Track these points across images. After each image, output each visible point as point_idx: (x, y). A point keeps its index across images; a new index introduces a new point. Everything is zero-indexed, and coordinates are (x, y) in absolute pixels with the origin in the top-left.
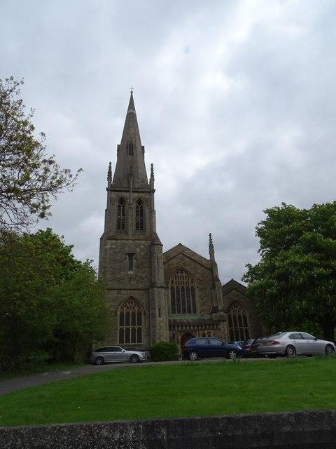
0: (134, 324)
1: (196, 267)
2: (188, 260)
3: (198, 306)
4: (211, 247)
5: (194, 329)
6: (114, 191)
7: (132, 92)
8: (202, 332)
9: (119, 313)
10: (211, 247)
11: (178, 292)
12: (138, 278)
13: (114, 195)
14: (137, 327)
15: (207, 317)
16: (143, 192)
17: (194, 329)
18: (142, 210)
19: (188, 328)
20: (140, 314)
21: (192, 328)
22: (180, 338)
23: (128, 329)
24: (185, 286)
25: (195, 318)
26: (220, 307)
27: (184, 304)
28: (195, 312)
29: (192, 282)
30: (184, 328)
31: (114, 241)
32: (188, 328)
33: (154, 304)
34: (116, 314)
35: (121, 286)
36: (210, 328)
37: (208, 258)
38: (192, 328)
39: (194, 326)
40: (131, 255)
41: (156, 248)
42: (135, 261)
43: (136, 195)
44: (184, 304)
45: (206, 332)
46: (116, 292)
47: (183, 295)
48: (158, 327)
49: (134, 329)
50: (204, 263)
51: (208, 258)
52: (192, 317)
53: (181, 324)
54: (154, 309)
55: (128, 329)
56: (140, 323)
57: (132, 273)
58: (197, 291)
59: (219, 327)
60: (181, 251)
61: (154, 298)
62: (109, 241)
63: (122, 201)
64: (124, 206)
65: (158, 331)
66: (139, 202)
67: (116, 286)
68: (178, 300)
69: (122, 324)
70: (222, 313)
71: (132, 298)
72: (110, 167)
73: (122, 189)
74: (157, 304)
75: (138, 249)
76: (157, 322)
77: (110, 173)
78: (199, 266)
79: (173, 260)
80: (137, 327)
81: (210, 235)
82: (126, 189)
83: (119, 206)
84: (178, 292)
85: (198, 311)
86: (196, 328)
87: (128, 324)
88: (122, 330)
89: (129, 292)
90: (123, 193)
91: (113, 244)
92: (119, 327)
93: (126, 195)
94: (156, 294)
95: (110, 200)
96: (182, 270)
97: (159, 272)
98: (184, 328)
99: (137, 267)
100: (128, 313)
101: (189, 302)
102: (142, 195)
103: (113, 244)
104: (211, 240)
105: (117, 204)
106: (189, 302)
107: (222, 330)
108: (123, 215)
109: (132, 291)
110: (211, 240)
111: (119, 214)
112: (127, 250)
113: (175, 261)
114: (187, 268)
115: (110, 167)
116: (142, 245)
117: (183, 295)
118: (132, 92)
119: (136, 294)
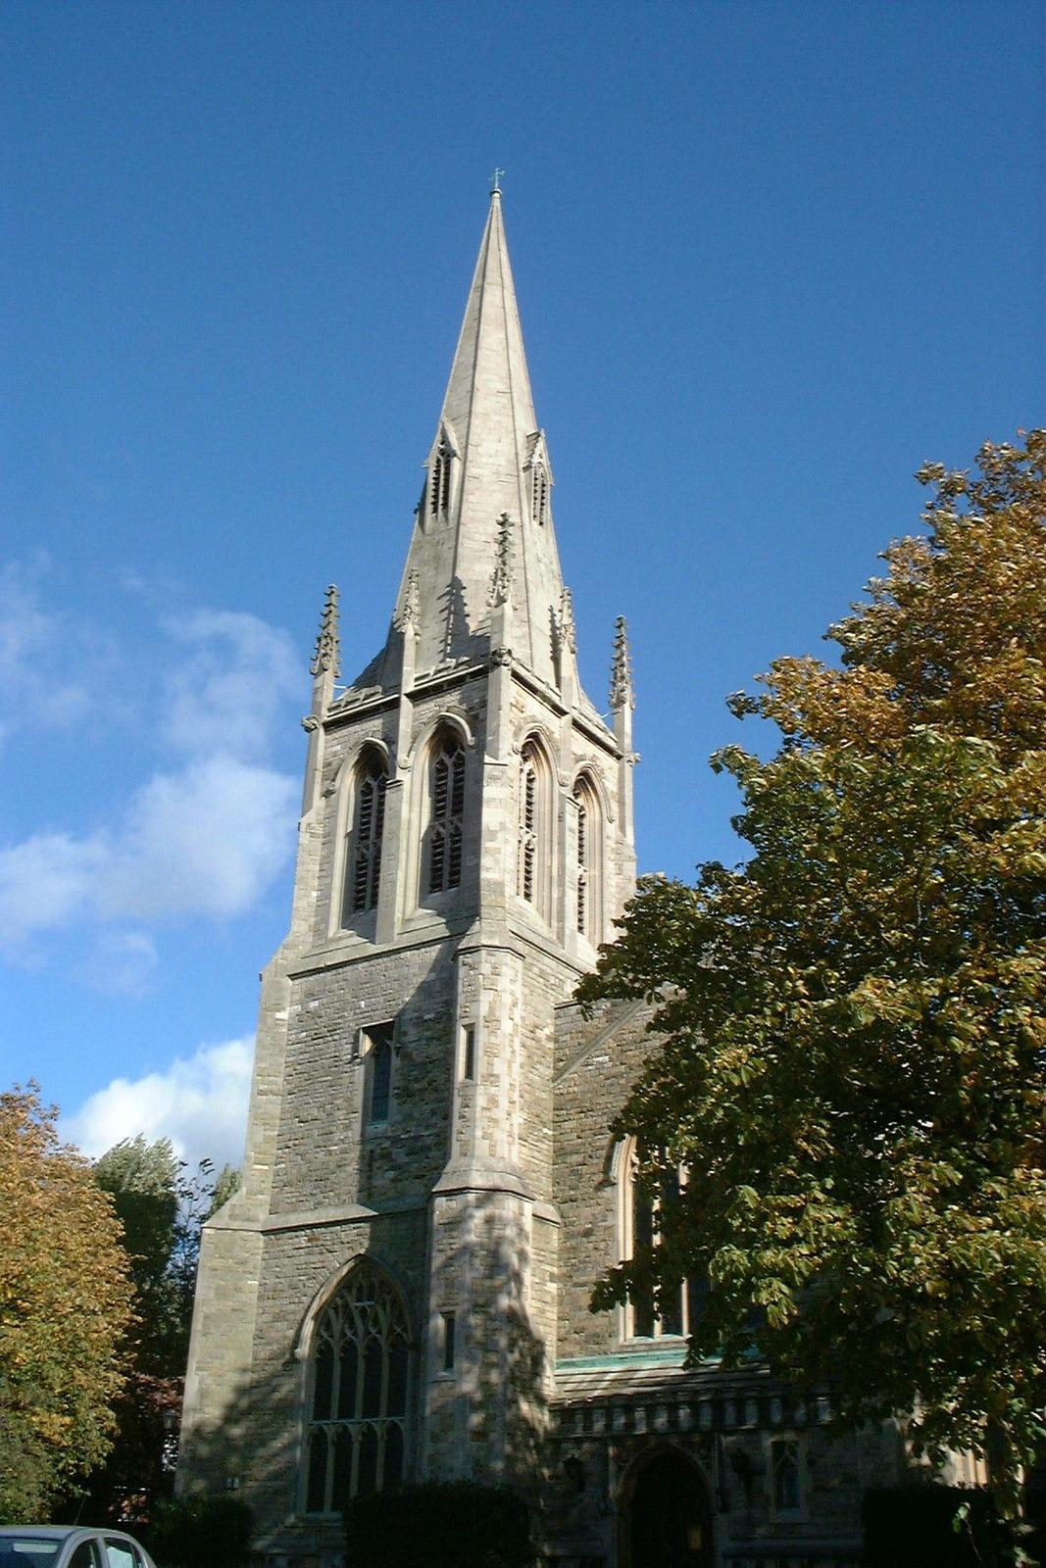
12: (399, 1154)
19: (661, 1421)
20: (397, 1343)
23: (344, 1437)
36: (788, 1422)
40: (378, 1033)
42: (396, 1062)
46: (302, 1239)
49: (369, 1435)
66: (445, 738)
91: (310, 995)
105: (348, 784)
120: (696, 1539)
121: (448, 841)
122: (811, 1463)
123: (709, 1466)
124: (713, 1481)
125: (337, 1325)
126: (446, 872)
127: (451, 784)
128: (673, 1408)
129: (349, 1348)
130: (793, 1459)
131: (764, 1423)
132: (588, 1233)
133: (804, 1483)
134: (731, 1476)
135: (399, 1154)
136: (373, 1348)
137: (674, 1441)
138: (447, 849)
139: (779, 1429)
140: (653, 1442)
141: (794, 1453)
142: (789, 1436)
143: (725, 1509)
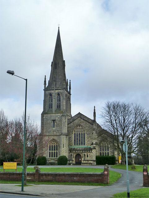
0: (54, 150)
1: (86, 124)
2: (83, 120)
3: (86, 141)
4: (95, 113)
6: (47, 90)
8: (84, 153)
9: (49, 145)
10: (95, 113)
11: (77, 135)
12: (56, 131)
14: (56, 151)
15: (89, 146)
16: (60, 89)
18: (60, 98)
20: (57, 146)
21: (80, 152)
22: (74, 156)
23: (52, 152)
24: (81, 133)
25: (84, 147)
26: (94, 143)
27: (80, 141)
28: (84, 144)
29: (84, 131)
30: (76, 152)
31: (47, 115)
33: (61, 142)
34: (48, 146)
35: (50, 134)
36: (88, 152)
37: (93, 119)
38: (80, 152)
39: (81, 151)
40: (54, 121)
42: (55, 123)
43: (57, 91)
44: (80, 141)
45: (86, 153)
47: (80, 137)
48: (62, 152)
49: (54, 152)
51: (93, 119)
52: (82, 147)
53: (76, 150)
54: (61, 144)
55: (52, 152)
56: (57, 150)
57: (54, 128)
58: (86, 134)
59: (92, 151)
60: (80, 115)
61: (61, 140)
62: (45, 115)
63: (51, 95)
64: (52, 97)
65: (62, 153)
66: (59, 94)
67: (47, 134)
68: (77, 139)
69: (50, 150)
70: (95, 145)
71: (54, 139)
74: (62, 142)
75: (57, 118)
76: (62, 150)
77: (45, 81)
78: (87, 123)
79: (76, 121)
80: (56, 151)
81: (95, 107)
82: (53, 89)
84: (77, 135)
85: (86, 144)
86: (82, 152)
87: (52, 150)
88: (50, 152)
89: (52, 137)
90: (51, 91)
91: (46, 116)
92: (49, 151)
93: (52, 91)
94: (62, 138)
95: (45, 95)
96: (79, 125)
97: (64, 128)
99: (57, 126)
100: (52, 146)
101: (82, 140)
102: (59, 91)
103: (46, 116)
104: (95, 109)
106: (82, 140)
108: (52, 101)
109: (54, 137)
110: (95, 109)
112: (53, 118)
113: (76, 121)
114: (82, 124)
116: (59, 116)
117: (80, 137)
119: (55, 138)
124: (82, 156)
125: (51, 144)
129: (52, 146)
131: (86, 152)
133: (89, 156)
134: (84, 155)
135: (56, 131)
136: (54, 146)
142: (88, 153)
143: (83, 157)
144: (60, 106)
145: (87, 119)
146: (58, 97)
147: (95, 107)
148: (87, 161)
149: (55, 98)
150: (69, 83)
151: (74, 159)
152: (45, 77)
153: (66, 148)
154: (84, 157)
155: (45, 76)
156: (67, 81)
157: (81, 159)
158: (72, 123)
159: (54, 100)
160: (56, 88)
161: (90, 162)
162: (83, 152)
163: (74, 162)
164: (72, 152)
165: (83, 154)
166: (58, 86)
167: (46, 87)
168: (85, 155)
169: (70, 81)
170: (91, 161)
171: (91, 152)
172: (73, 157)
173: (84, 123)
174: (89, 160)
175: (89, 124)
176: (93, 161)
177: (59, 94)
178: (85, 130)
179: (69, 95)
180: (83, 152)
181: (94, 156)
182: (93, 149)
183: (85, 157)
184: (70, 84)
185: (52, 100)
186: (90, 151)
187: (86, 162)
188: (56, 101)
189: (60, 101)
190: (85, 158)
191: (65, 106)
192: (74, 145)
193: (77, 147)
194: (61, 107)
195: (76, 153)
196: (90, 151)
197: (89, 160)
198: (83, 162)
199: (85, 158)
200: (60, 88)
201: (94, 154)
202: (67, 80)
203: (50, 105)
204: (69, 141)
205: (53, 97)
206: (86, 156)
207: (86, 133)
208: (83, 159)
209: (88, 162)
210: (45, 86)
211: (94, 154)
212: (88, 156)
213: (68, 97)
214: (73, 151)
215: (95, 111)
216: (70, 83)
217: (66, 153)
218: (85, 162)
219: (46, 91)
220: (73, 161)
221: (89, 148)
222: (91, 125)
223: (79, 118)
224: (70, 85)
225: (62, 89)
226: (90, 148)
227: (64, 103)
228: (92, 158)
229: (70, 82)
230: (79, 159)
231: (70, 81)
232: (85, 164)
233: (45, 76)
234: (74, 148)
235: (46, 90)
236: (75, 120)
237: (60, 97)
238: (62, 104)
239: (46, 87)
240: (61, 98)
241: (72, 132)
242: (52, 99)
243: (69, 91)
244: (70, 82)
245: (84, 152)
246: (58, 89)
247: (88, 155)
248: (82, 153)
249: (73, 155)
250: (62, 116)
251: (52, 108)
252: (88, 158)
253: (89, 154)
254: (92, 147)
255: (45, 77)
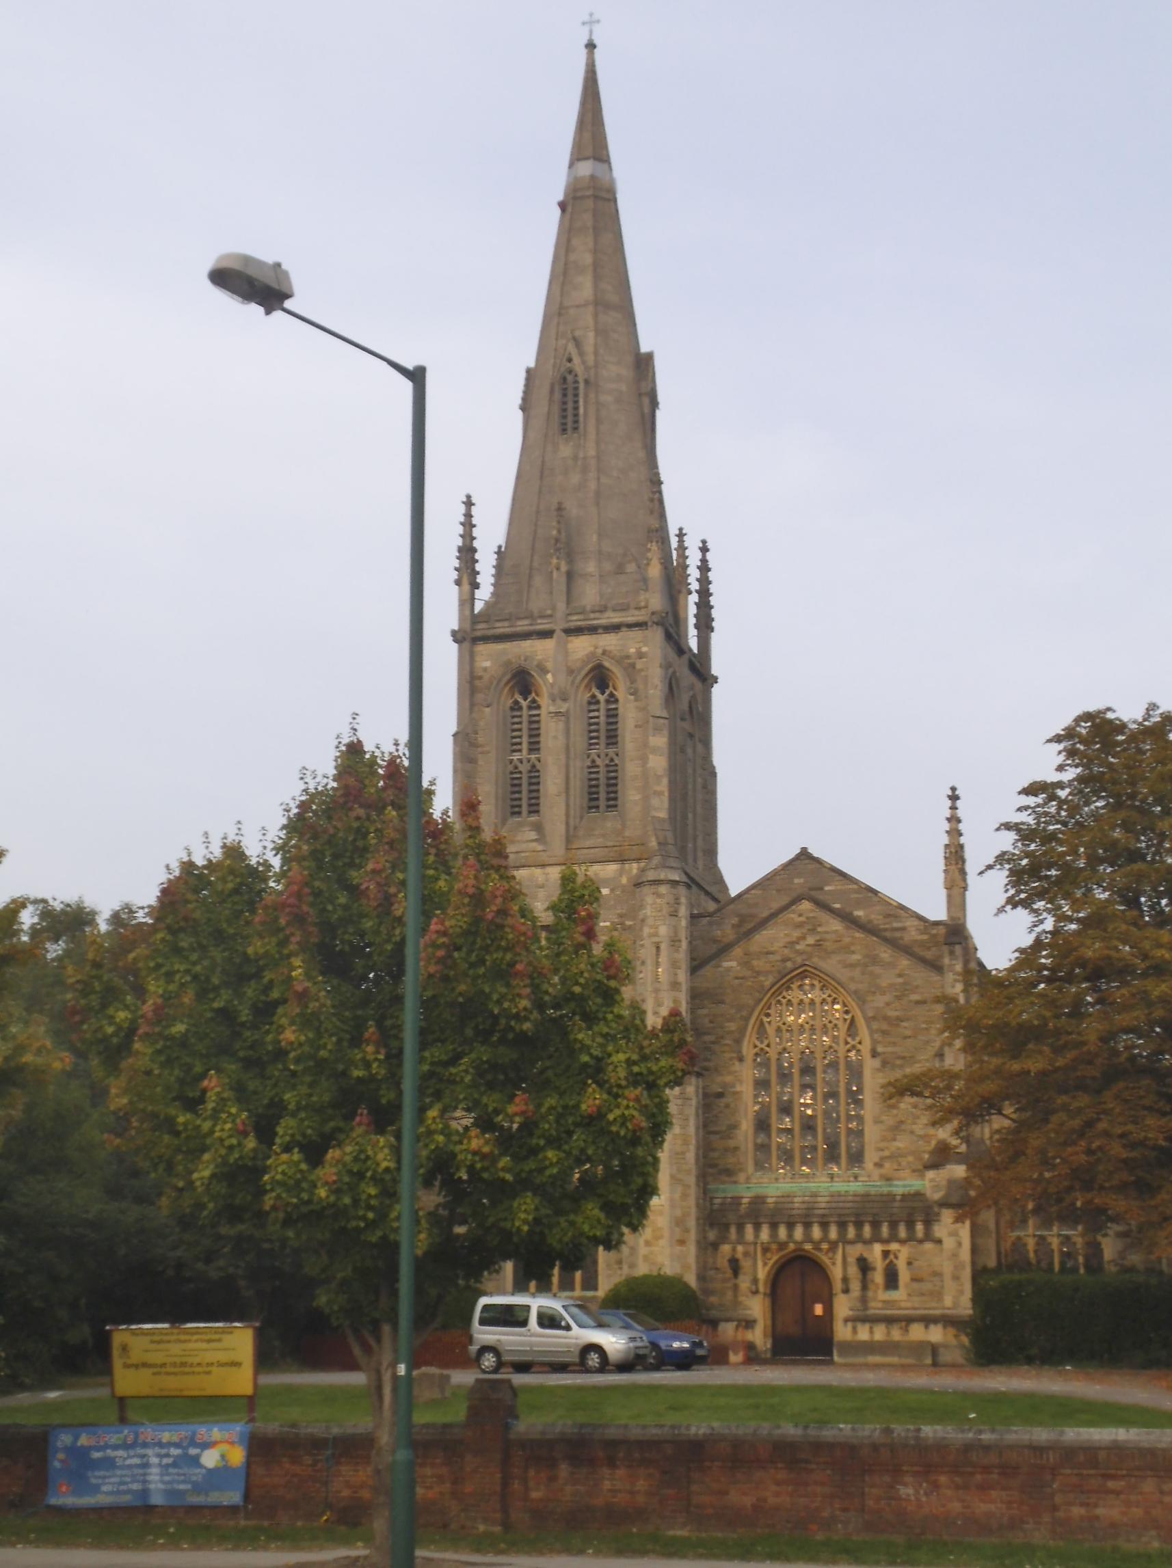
1: (874, 960)
2: (836, 925)
3: (872, 1134)
5: (825, 1238)
6: (486, 639)
7: (591, 46)
8: (856, 1250)
13: (488, 658)
15: (907, 1183)
17: (825, 1238)
18: (612, 715)
19: (799, 1233)
21: (816, 1232)
22: (762, 1273)
25: (855, 1187)
28: (857, 1158)
30: (782, 1232)
32: (799, 1233)
36: (893, 1237)
38: (816, 1232)
39: (824, 1226)
41: (649, 899)
43: (581, 646)
45: (878, 1248)
50: (912, 934)
51: (935, 909)
52: (839, 1186)
59: (939, 1230)
64: (535, 705)
66: (600, 678)
72: (468, 524)
73: (523, 626)
78: (885, 954)
81: (954, 797)
82: (543, 625)
83: (516, 706)
85: (871, 1157)
86: (833, 1233)
90: (527, 645)
93: (541, 649)
98: (782, 1232)
102: (609, 641)
104: (954, 819)
107: (949, 1243)
108: (534, 747)
110: (954, 819)
111: (515, 747)
113: (774, 937)
114: (831, 965)
115: (468, 524)
118: (591, 46)
120: (819, 1310)
121: (602, 770)
122: (909, 1263)
123: (834, 1264)
124: (837, 1273)
126: (603, 796)
127: (603, 719)
128: (807, 1226)
130: (895, 1261)
131: (876, 1238)
132: (720, 1095)
133: (904, 1275)
134: (853, 1271)
137: (808, 1247)
138: (602, 776)
139: (887, 1241)
140: (792, 1246)
141: (896, 1257)
142: (894, 1246)
143: (846, 1291)
144: (613, 784)
145: (876, 918)
146: (593, 701)
147: (954, 797)
148: (890, 1321)
149: (566, 715)
150: (694, 573)
151: (757, 1308)
152: (468, 515)
153: (684, 1196)
154: (855, 1286)
155: (469, 503)
156: (682, 548)
157: (829, 1309)
158: (738, 951)
159: (552, 733)
160: (576, 621)
161: (917, 1332)
162: (851, 1232)
163: (759, 1337)
164: (741, 1240)
165: (851, 1260)
166: (590, 594)
167: (479, 606)
168: (864, 1266)
169: (704, 549)
170: (928, 1321)
171: (928, 1237)
172: (744, 1283)
173: (847, 949)
174: (910, 1320)
175: (904, 962)
176: (948, 1321)
177: (600, 678)
178: (861, 1022)
179: (699, 685)
180: (843, 1239)
181: (956, 1278)
182: (944, 1204)
183: (865, 1287)
184: (704, 582)
185: (535, 734)
186: (920, 1227)
187: (880, 1333)
188: (580, 742)
189: (612, 738)
190: (864, 1300)
191: (664, 786)
192: (750, 1167)
193: (785, 1187)
194: (631, 796)
195: (782, 1246)
196: (920, 1227)
197: (910, 1320)
198: (842, 1332)
199: (864, 1300)
200: (616, 618)
201: (955, 1255)
202: (681, 535)
203: (515, 786)
204: (705, 1126)
205: (544, 701)
206: (878, 1277)
207: (874, 1054)
208: (843, 1306)
209: (896, 1334)
210: (467, 601)
211: (955, 1255)
212: (892, 1280)
213: (685, 706)
214: (749, 1229)
215: (955, 833)
216: (704, 567)
217: (682, 1242)
218: (863, 1334)
219: (481, 648)
220: (749, 1324)
221: (905, 1197)
222: (920, 975)
223: (806, 905)
224: (704, 593)
225: (630, 626)
226: (918, 1195)
227: (658, 763)
228: (938, 1295)
229: (704, 561)
230: (806, 1310)
231: (704, 549)
232: (872, 1359)
233: (469, 503)
234: (759, 1200)
235: (475, 640)
236: (763, 923)
237: (612, 699)
238: (631, 769)
239: (479, 606)
240: (629, 714)
241: (738, 1041)
242: (534, 723)
243: (693, 644)
244: (704, 561)
245: (859, 1239)
246: (593, 630)
247: (901, 1264)
248: (833, 1246)
249: (746, 1264)
250: (638, 885)
251: (534, 809)
252: (899, 1295)
253: (903, 1253)
254: (932, 1184)
255: (468, 515)
